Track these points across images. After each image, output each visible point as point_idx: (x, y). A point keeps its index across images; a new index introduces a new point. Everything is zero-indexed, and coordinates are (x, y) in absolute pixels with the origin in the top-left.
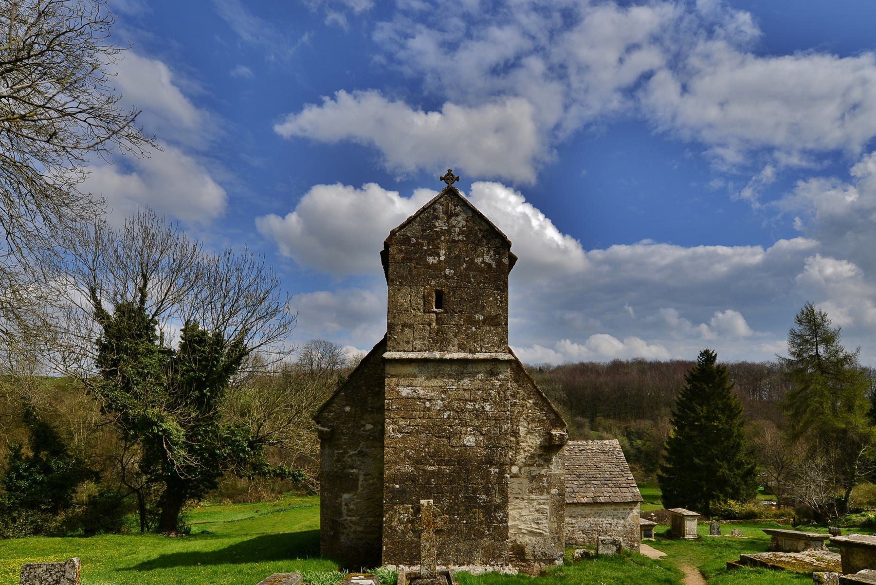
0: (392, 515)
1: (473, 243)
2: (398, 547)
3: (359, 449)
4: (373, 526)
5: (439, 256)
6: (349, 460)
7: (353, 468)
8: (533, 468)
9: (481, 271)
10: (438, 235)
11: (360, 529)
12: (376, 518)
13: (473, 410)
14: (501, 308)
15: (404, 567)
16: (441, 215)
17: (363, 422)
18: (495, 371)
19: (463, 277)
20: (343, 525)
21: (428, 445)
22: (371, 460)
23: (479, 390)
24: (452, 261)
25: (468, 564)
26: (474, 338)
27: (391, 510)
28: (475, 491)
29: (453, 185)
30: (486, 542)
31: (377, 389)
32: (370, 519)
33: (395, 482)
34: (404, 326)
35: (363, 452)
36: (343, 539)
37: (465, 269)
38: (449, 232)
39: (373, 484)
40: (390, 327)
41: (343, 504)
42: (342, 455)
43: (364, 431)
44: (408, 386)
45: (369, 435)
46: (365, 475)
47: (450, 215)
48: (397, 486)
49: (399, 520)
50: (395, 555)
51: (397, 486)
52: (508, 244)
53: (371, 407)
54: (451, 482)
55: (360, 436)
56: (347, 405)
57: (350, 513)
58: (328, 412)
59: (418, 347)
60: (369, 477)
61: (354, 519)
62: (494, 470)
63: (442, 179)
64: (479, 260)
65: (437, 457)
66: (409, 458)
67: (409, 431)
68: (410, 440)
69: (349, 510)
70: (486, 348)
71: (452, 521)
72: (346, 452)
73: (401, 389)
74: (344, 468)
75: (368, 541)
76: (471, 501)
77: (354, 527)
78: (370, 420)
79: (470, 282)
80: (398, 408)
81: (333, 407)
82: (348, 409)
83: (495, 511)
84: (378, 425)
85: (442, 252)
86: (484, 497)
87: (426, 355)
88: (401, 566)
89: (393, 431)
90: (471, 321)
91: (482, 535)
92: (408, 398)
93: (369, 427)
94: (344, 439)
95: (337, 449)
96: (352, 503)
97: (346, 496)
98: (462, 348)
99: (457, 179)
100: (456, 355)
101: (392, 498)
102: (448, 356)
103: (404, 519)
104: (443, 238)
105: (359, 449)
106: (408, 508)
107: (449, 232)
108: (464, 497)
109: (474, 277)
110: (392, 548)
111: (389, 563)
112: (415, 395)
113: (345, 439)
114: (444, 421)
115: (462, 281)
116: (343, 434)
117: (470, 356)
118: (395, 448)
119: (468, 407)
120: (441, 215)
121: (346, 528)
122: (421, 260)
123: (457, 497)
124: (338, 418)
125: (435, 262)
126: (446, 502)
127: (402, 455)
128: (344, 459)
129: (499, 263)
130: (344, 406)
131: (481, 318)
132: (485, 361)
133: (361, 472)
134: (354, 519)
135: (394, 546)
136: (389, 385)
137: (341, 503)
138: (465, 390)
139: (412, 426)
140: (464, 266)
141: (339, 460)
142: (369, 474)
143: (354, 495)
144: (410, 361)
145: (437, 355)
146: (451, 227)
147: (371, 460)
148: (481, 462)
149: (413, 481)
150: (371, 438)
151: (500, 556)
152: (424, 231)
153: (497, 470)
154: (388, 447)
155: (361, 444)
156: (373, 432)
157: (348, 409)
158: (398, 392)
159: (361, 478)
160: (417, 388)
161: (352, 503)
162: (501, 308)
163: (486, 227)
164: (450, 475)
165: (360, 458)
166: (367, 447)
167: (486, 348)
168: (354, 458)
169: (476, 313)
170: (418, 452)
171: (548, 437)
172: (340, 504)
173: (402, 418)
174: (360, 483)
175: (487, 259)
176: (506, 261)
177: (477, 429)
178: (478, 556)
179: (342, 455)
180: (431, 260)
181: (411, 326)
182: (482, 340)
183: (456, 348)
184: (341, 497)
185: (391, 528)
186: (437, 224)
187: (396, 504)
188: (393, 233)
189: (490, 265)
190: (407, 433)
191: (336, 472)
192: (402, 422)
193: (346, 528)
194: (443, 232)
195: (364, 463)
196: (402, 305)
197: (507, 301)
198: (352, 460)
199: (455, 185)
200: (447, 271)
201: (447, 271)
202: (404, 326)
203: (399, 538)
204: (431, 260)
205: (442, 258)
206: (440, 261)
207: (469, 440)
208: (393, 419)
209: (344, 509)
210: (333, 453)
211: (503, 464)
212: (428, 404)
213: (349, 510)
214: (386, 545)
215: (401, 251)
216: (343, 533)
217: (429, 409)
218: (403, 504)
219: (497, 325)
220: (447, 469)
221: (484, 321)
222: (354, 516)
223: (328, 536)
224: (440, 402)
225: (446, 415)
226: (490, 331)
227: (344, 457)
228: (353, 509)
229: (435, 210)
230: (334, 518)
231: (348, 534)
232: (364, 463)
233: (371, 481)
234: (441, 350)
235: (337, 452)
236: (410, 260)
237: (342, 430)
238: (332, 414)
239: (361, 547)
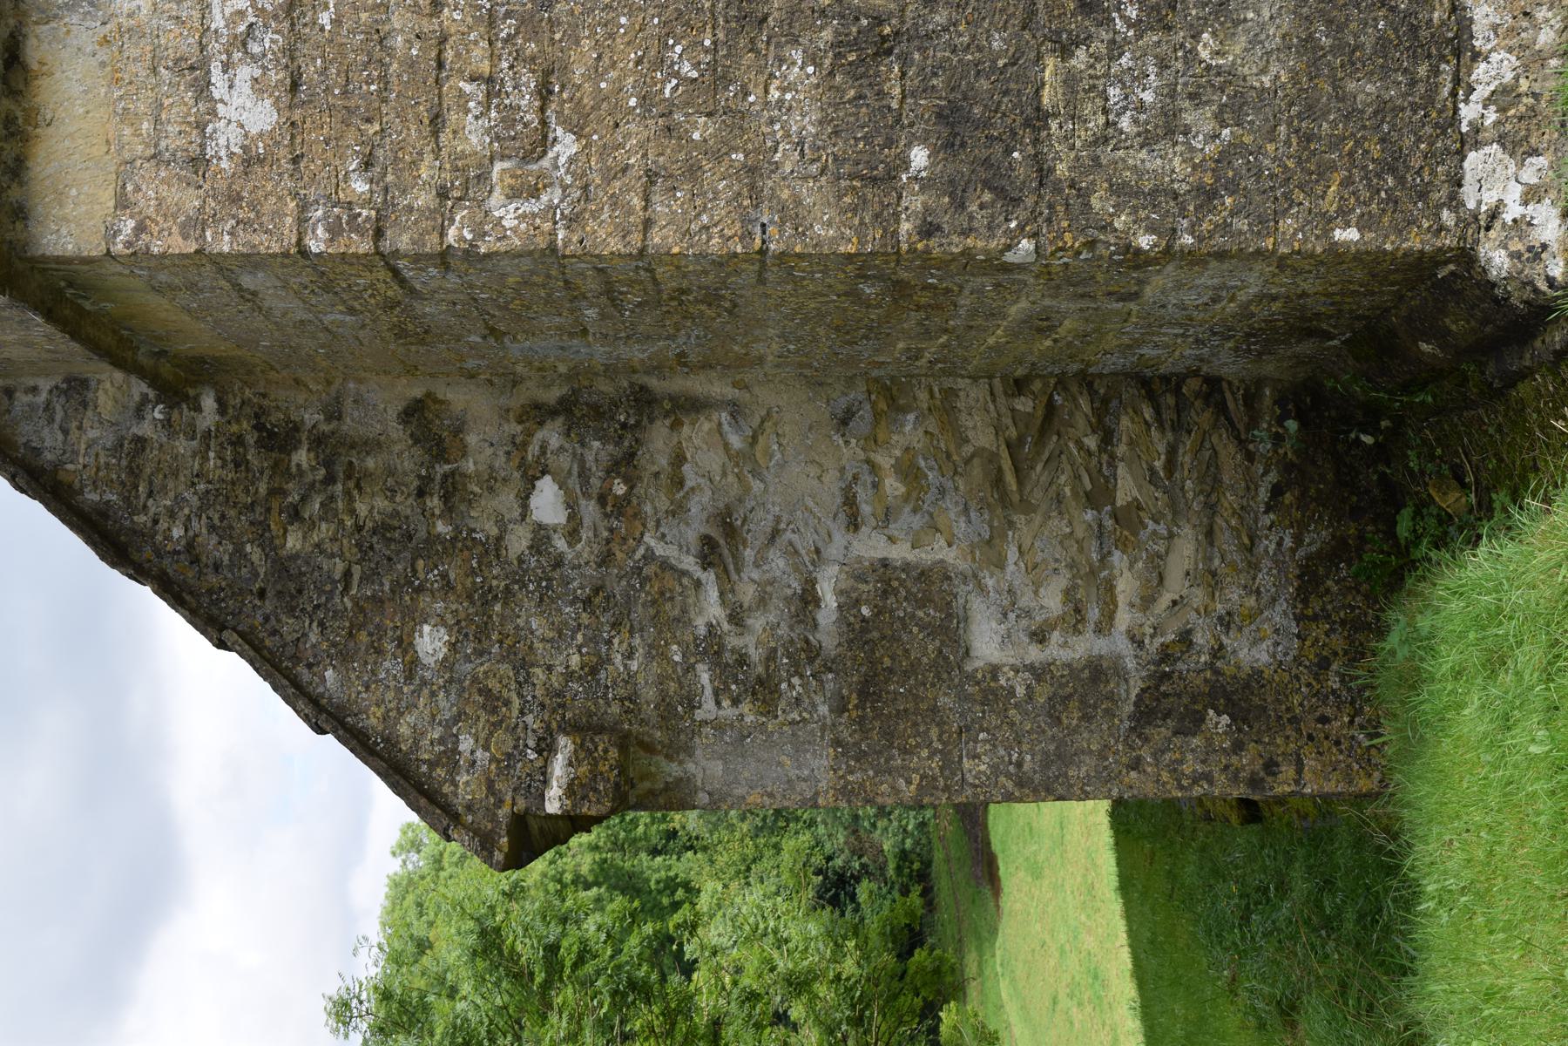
0: (1119, 190)
2: (1336, 143)
3: (689, 563)
4: (1170, 465)
6: (757, 622)
7: (808, 599)
11: (1185, 552)
12: (1122, 449)
15: (1482, 92)
17: (518, 542)
20: (1165, 655)
22: (757, 486)
27: (1084, 194)
31: (302, 457)
33: (891, 176)
35: (707, 541)
39: (909, 472)
41: (1034, 654)
42: (730, 668)
43: (573, 535)
44: (202, 88)
45: (602, 500)
46: (854, 524)
48: (919, 157)
49: (1147, 140)
50: (1394, 164)
51: (919, 157)
53: (421, 493)
55: (606, 559)
56: (405, 645)
57: (1094, 614)
58: (454, 768)
60: (863, 494)
61: (1126, 586)
66: (724, 80)
67: (530, 81)
68: (596, 73)
69: (1075, 617)
72: (711, 647)
73: (225, 140)
74: (812, 652)
75: (1263, 494)
77: (1176, 585)
78: (506, 500)
80: (367, 164)
81: (418, 735)
82: (431, 643)
84: (533, 450)
88: (1468, 112)
89: (535, 193)
92: (295, 86)
93: (547, 503)
95: (692, 704)
96: (1025, 600)
101: (1000, 192)
103: (1141, 107)
105: (689, 563)
106: (1070, 81)
110: (1347, 182)
111: (1455, 202)
112: (269, 41)
113: (629, 655)
118: (651, 176)
121: (1185, 638)
124: (492, 702)
127: (701, 130)
128: (755, 655)
130: (412, 666)
133: (834, 551)
135: (1333, 167)
136: (196, 224)
137: (1031, 668)
139: (494, 58)
141: (764, 691)
142: (850, 501)
143: (982, 589)
147: (757, 486)
149: (883, 49)
150: (620, 489)
154: (648, 224)
155: (660, 550)
156: (584, 475)
157: (431, 643)
158: (249, 161)
159: (871, 546)
160: (218, 22)
161: (1025, 600)
165: (749, 554)
166: (678, 511)
168: (747, 593)
172: (1039, 672)
173: (435, 134)
174: (900, 553)
179: (730, 668)
184: (994, 671)
185: (1208, 197)
187: (1043, 173)
190: (544, 93)
191: (840, 708)
193: (1185, 638)
195: (775, 534)
198: (762, 601)
203: (1272, 136)
208: (443, 194)
210: (719, 727)
213: (1075, 617)
214: (1328, 222)
216: (1218, 651)
218: (1038, 119)
222: (1110, 587)
223: (1238, 747)
227: (742, 660)
228: (1068, 593)
230: (1129, 708)
231: (1226, 622)
232: (775, 534)
233: (893, 486)
235: (709, 704)
237: (569, 675)
238: (466, 744)
239: (1298, 540)
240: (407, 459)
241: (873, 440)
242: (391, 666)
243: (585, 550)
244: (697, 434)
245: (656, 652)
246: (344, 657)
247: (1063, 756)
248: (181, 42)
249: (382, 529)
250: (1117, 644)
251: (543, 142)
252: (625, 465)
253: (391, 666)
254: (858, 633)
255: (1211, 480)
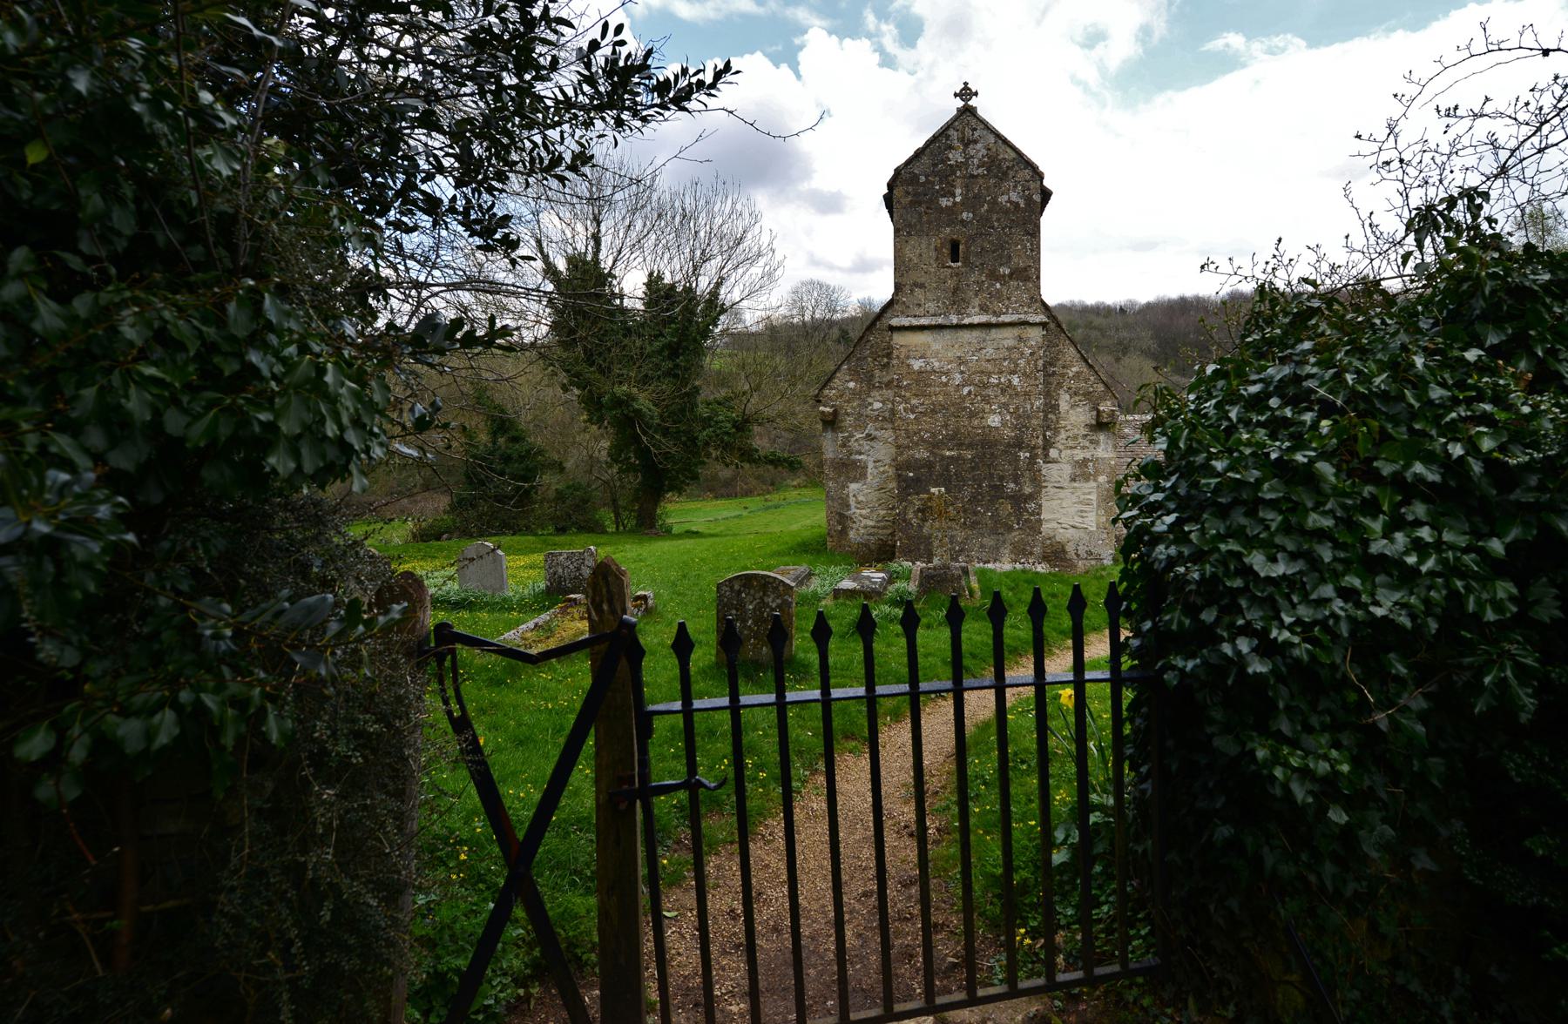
0: (906, 507)
1: (997, 177)
5: (954, 196)
7: (861, 454)
8: (1076, 452)
9: (1007, 212)
10: (952, 170)
11: (871, 523)
13: (997, 385)
14: (1032, 258)
16: (956, 143)
17: (870, 400)
18: (1024, 336)
19: (984, 221)
21: (946, 426)
23: (1005, 359)
24: (971, 202)
25: (995, 561)
26: (998, 296)
28: (1001, 478)
29: (970, 103)
30: (1015, 536)
32: (882, 513)
34: (916, 285)
36: (852, 534)
37: (987, 211)
38: (965, 164)
39: (884, 472)
40: (898, 287)
42: (847, 439)
47: (967, 143)
50: (910, 551)
52: (1041, 176)
54: (973, 469)
59: (932, 311)
61: (864, 512)
62: (1024, 455)
63: (956, 95)
64: (1003, 199)
65: (956, 440)
70: (1013, 309)
71: (976, 513)
73: (912, 362)
76: (997, 491)
79: (993, 227)
82: (852, 385)
83: (1025, 502)
85: (958, 191)
86: (1012, 485)
87: (940, 320)
90: (994, 276)
91: (1010, 529)
93: (877, 405)
94: (849, 420)
97: (853, 486)
98: (984, 309)
99: (976, 94)
100: (976, 320)
102: (967, 321)
104: (958, 173)
107: (965, 164)
108: (989, 486)
109: (998, 220)
112: (929, 368)
114: (963, 398)
115: (984, 226)
116: (848, 415)
117: (994, 320)
119: (992, 380)
120: (956, 143)
122: (932, 203)
123: (980, 486)
124: (841, 396)
125: (950, 204)
126: (967, 492)
129: (1029, 200)
131: (1007, 271)
132: (1011, 324)
134: (864, 512)
136: (898, 357)
138: (988, 361)
140: (986, 206)
141: (844, 445)
144: (922, 328)
145: (954, 320)
146: (968, 158)
148: (1009, 445)
151: (1031, 553)
152: (935, 165)
153: (1028, 455)
157: (852, 385)
159: (871, 465)
162: (1032, 258)
163: (1013, 155)
164: (972, 460)
166: (876, 429)
167: (1013, 309)
169: (1001, 265)
170: (934, 435)
171: (1094, 413)
172: (848, 496)
174: (869, 471)
175: (1014, 197)
176: (1037, 198)
177: (1005, 406)
178: (1006, 552)
180: (945, 202)
181: (922, 286)
182: (1009, 299)
183: (977, 309)
185: (904, 521)
186: (951, 156)
188: (898, 171)
189: (1017, 204)
192: (914, 401)
194: (959, 166)
196: (910, 260)
197: (1039, 248)
199: (973, 102)
200: (965, 215)
201: (965, 215)
202: (916, 285)
204: (945, 202)
205: (958, 199)
206: (955, 203)
207: (994, 420)
209: (852, 501)
211: (1034, 448)
212: (944, 379)
215: (908, 193)
217: (946, 385)
218: (918, 494)
219: (1027, 279)
220: (968, 455)
221: (1011, 276)
224: (958, 376)
225: (966, 391)
226: (1018, 288)
229: (948, 137)
233: (882, 469)
234: (959, 313)
236: (920, 204)
240: (885, 380)
241: (890, 465)
242: (848, 378)
243: (869, 412)
244: (890, 432)
245: (850, 426)
246: (849, 369)
247: (833, 500)
248: (928, 354)
249: (872, 375)
250: (853, 510)
251: (913, 412)
252: (885, 419)
253: (848, 378)
254: (855, 462)
255: (884, 528)
